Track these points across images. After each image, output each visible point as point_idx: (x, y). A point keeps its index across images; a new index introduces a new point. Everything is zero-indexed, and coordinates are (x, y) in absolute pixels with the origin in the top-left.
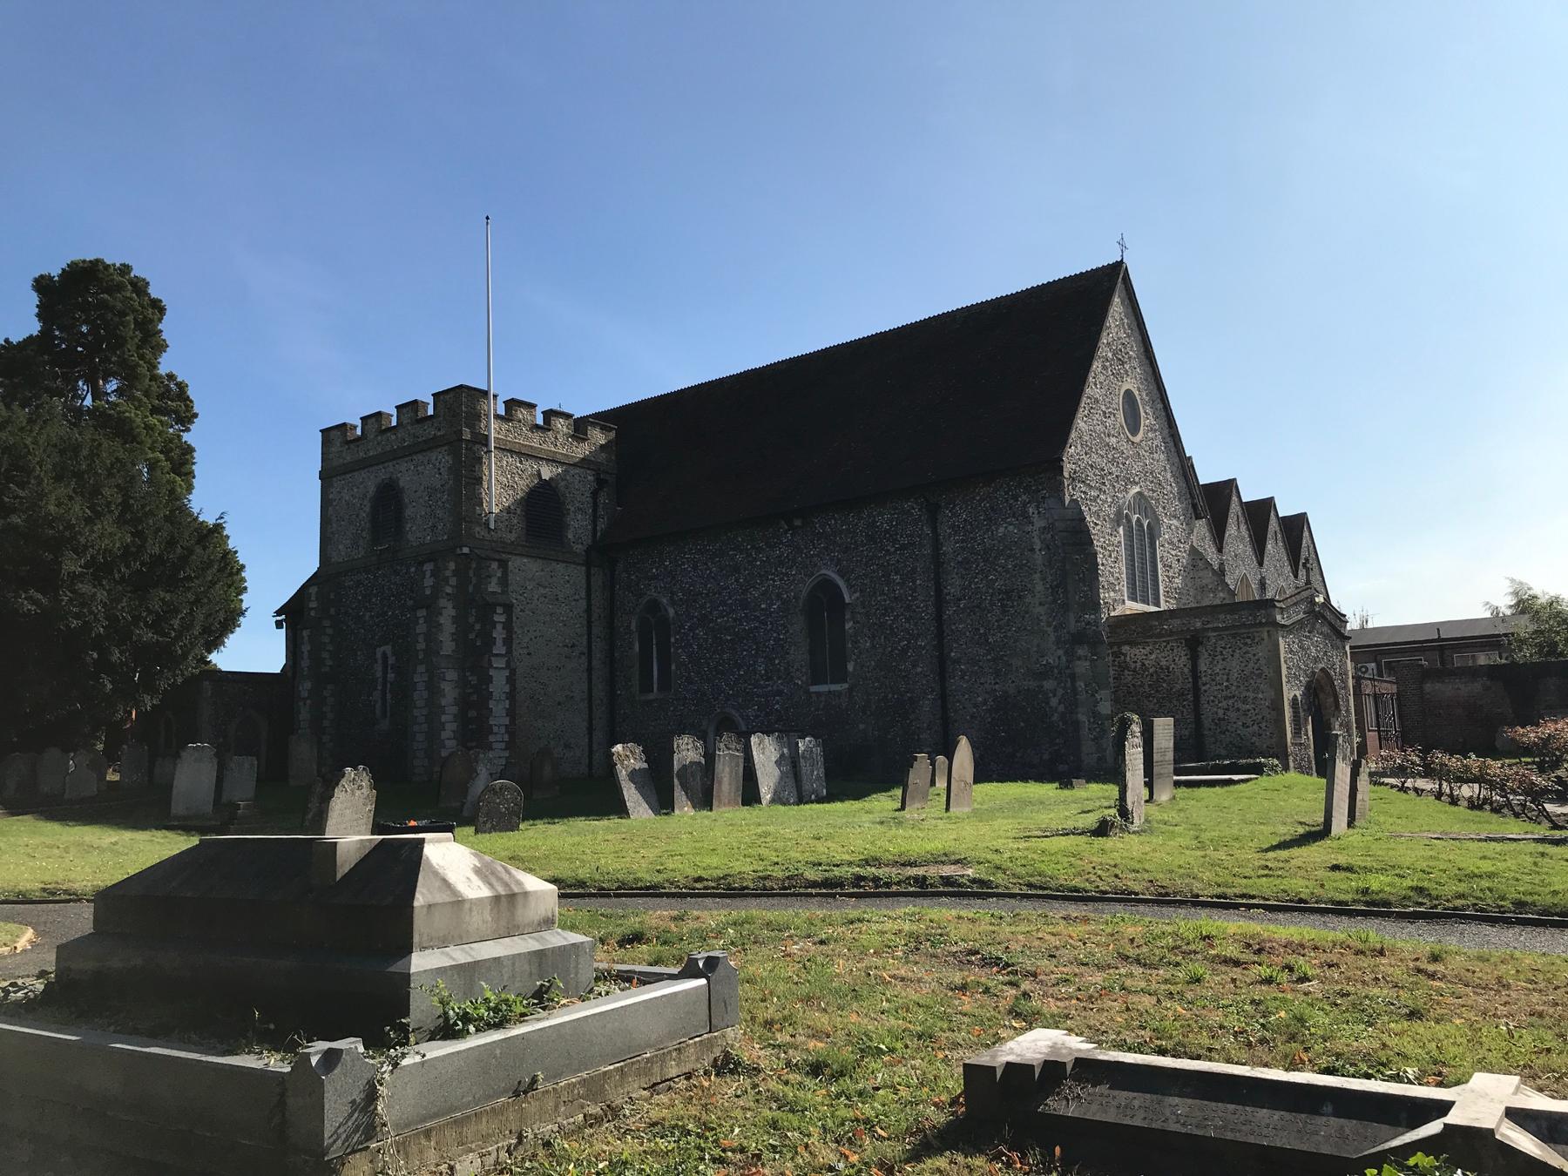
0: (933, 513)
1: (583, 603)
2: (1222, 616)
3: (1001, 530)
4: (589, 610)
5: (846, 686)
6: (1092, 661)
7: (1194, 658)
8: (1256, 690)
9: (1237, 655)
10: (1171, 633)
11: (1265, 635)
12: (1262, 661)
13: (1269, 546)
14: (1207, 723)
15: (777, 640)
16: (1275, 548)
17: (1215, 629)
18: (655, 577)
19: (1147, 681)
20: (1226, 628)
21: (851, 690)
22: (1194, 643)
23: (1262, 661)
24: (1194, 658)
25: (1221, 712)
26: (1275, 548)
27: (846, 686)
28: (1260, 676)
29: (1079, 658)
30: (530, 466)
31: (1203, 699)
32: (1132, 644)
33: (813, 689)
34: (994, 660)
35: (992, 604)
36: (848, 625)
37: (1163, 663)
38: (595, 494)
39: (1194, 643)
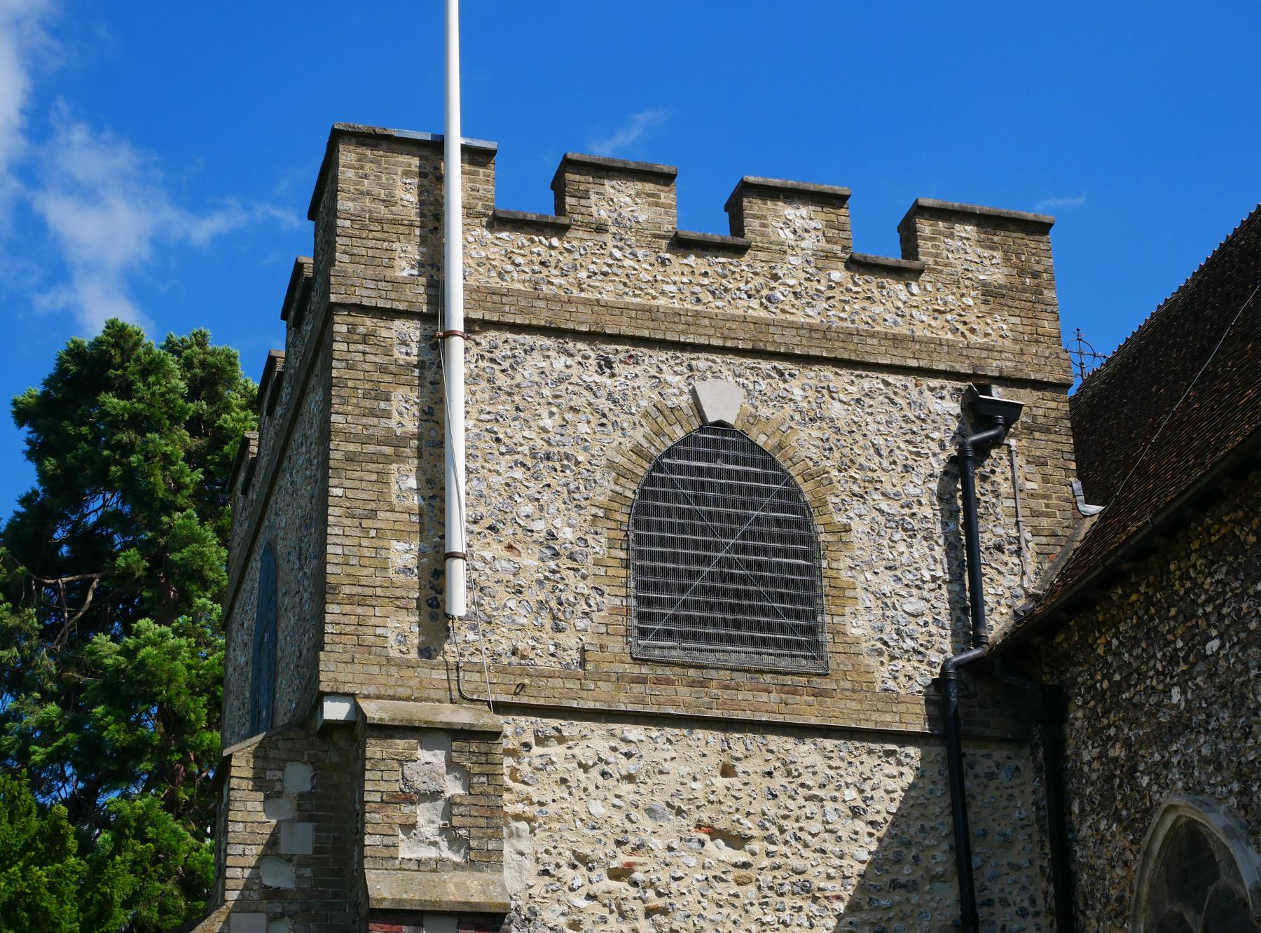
1: (950, 894)
18: (1180, 725)
30: (652, 382)
38: (963, 468)
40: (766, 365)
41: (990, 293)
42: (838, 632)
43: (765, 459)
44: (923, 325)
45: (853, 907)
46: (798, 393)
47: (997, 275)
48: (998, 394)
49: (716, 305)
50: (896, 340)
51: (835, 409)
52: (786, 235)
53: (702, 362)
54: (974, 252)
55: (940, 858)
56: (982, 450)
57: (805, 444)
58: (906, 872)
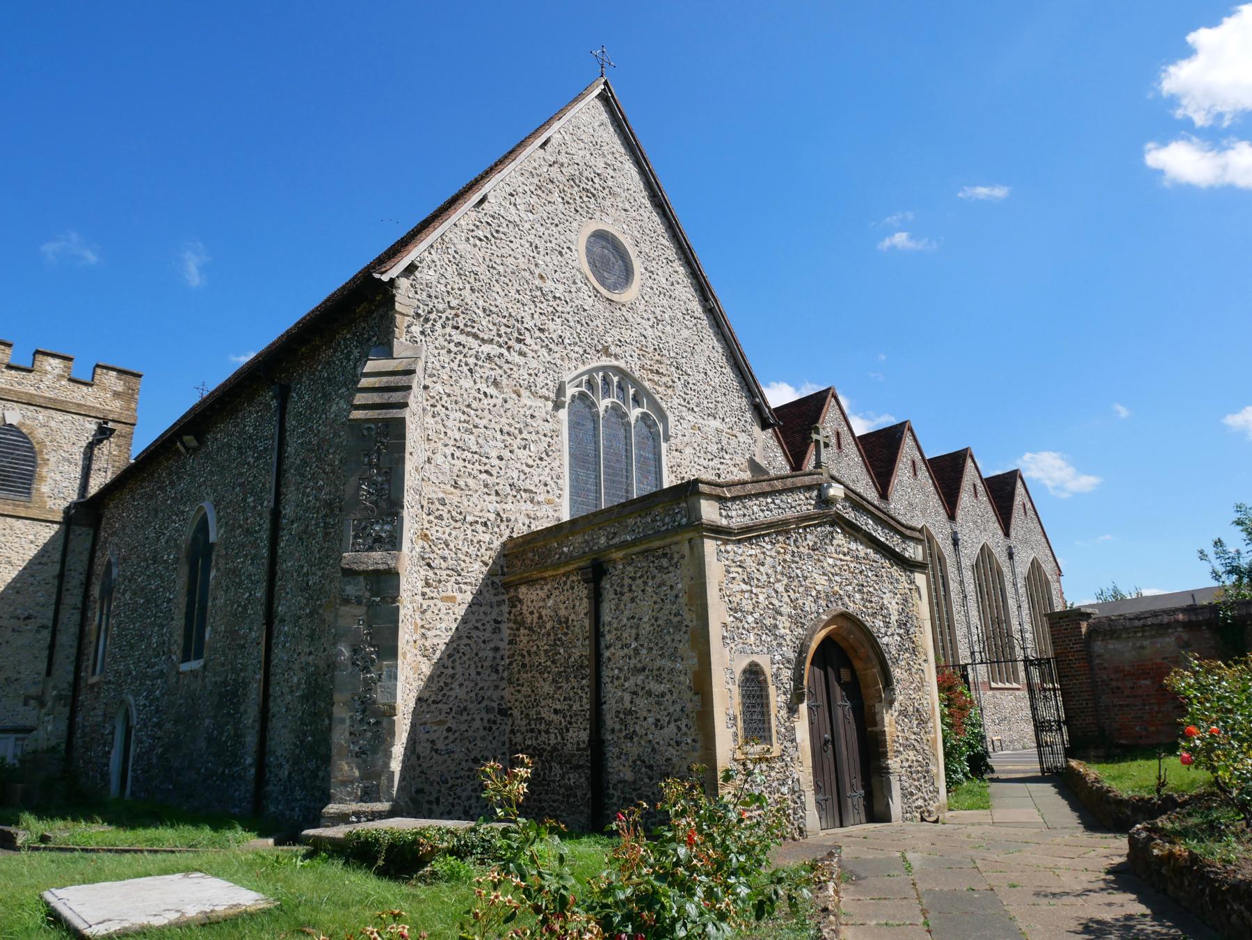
0: (283, 396)
1: (57, 567)
2: (631, 521)
3: (334, 408)
4: (61, 576)
5: (201, 662)
6: (371, 605)
7: (596, 598)
8: (674, 656)
9: (649, 590)
10: (570, 559)
11: (686, 548)
12: (683, 600)
13: (965, 498)
14: (610, 721)
15: (170, 601)
16: (974, 504)
17: (624, 545)
19: (543, 644)
20: (633, 543)
21: (205, 667)
22: (596, 572)
23: (683, 600)
24: (596, 598)
25: (627, 697)
26: (974, 504)
27: (201, 662)
28: (678, 627)
29: (346, 601)
31: (606, 673)
32: (530, 582)
33: (185, 667)
34: (311, 614)
35: (317, 525)
36: (213, 573)
37: (563, 612)
38: (91, 447)
39: (596, 572)
40: (31, 408)
41: (116, 394)
42: (38, 490)
43: (24, 436)
44: (91, 401)
45: (25, 569)
46: (41, 417)
47: (120, 389)
48: (110, 425)
49: (17, 388)
50: (79, 405)
51: (53, 424)
52: (49, 368)
53: (9, 404)
54: (113, 380)
55: (57, 556)
56: (100, 441)
57: (40, 433)
58: (45, 560)
